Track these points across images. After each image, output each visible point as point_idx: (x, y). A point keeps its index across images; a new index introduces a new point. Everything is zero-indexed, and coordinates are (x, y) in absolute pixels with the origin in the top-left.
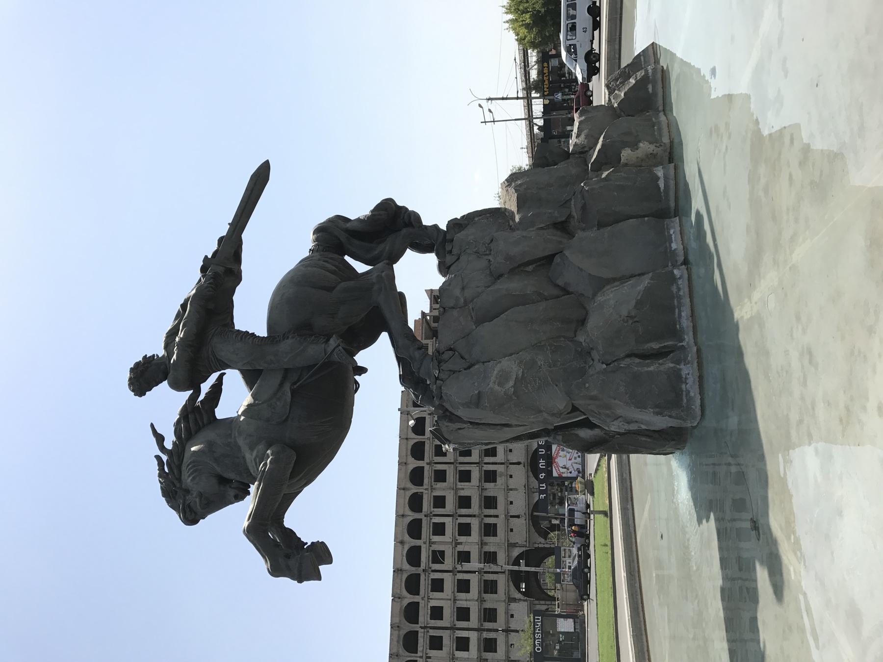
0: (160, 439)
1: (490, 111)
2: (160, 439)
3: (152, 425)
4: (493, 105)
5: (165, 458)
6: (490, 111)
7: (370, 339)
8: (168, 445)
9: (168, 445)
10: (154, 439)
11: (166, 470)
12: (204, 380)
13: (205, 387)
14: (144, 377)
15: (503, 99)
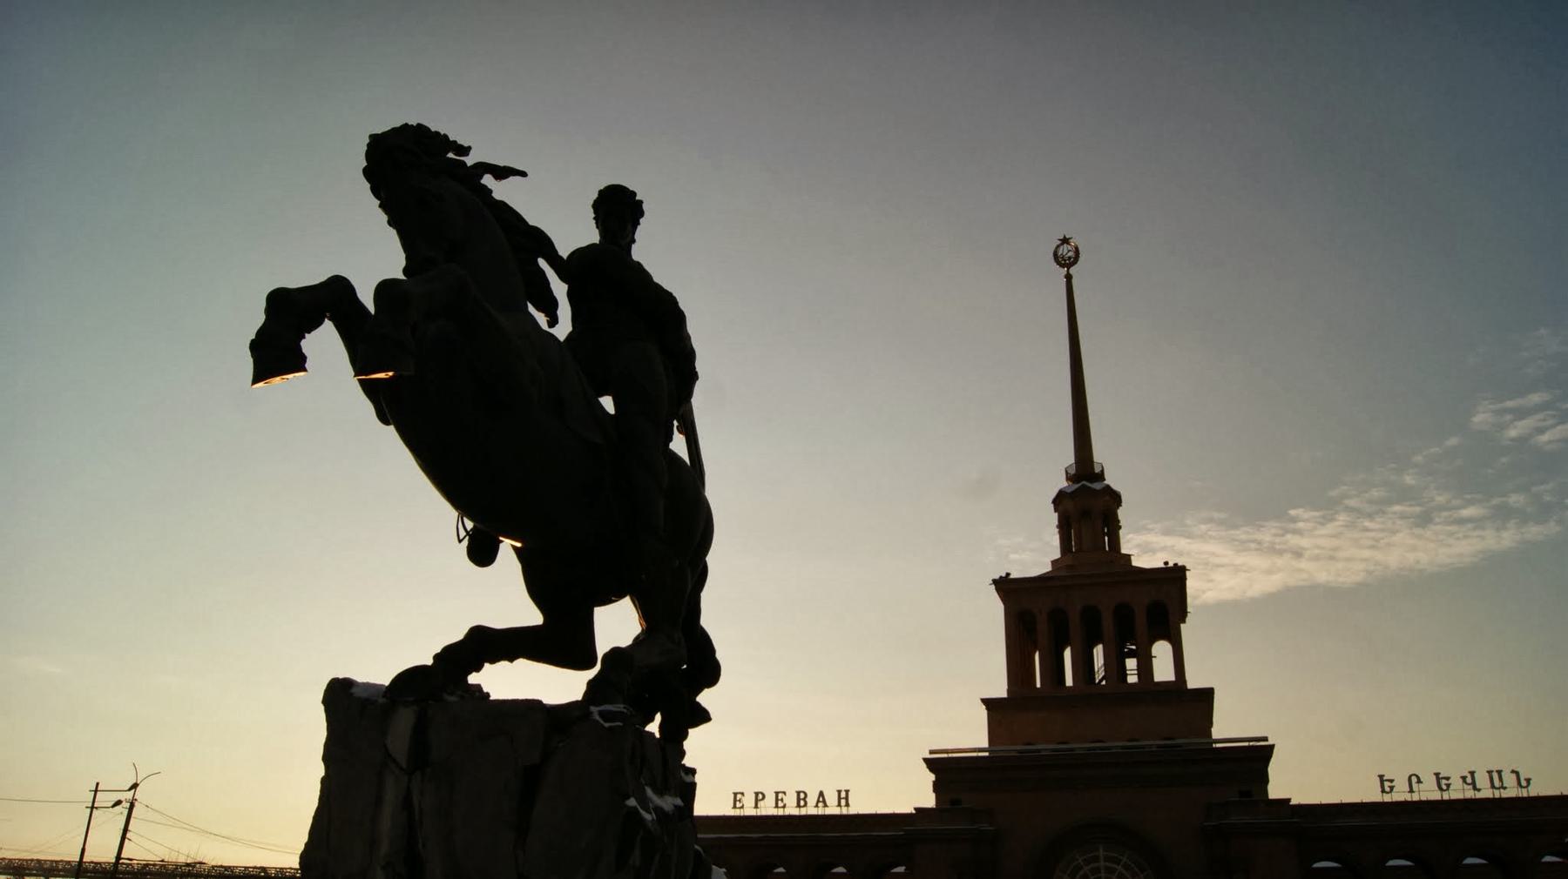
0: (502, 173)
1: (118, 803)
2: (502, 173)
3: (523, 174)
4: (122, 810)
5: (470, 161)
6: (118, 803)
7: (537, 588)
8: (488, 180)
9: (488, 180)
10: (502, 164)
11: (450, 155)
12: (570, 295)
13: (559, 289)
14: (618, 210)
15: (126, 830)
